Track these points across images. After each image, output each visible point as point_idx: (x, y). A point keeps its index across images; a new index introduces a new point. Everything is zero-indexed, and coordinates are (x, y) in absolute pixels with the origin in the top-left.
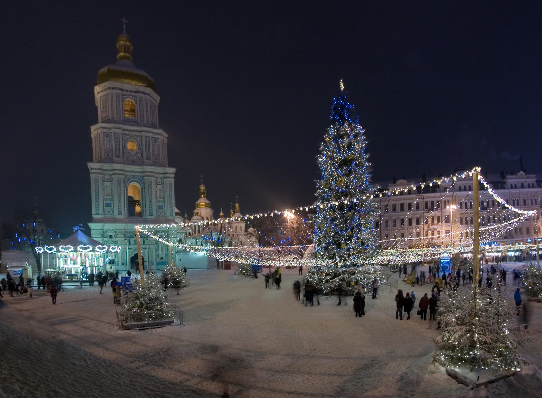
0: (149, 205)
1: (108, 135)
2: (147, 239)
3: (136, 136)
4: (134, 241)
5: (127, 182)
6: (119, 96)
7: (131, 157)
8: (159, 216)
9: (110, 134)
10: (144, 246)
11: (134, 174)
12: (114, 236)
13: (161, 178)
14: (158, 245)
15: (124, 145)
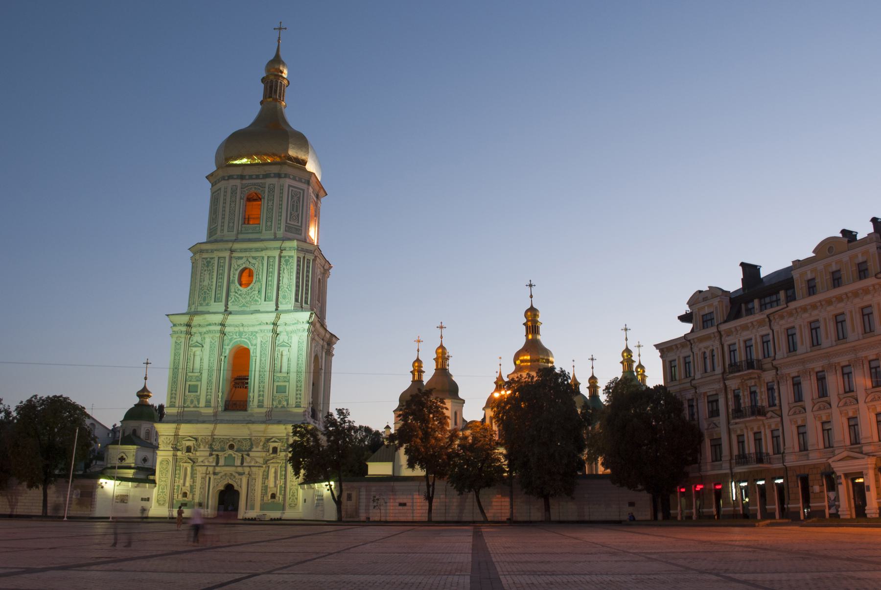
0: (259, 388)
1: (210, 262)
2: (248, 455)
3: (254, 258)
4: (225, 457)
5: (228, 345)
6: (237, 189)
7: (240, 299)
8: (276, 407)
9: (212, 261)
10: (240, 470)
11: (241, 329)
12: (194, 447)
13: (287, 332)
14: (269, 467)
15: (231, 278)
